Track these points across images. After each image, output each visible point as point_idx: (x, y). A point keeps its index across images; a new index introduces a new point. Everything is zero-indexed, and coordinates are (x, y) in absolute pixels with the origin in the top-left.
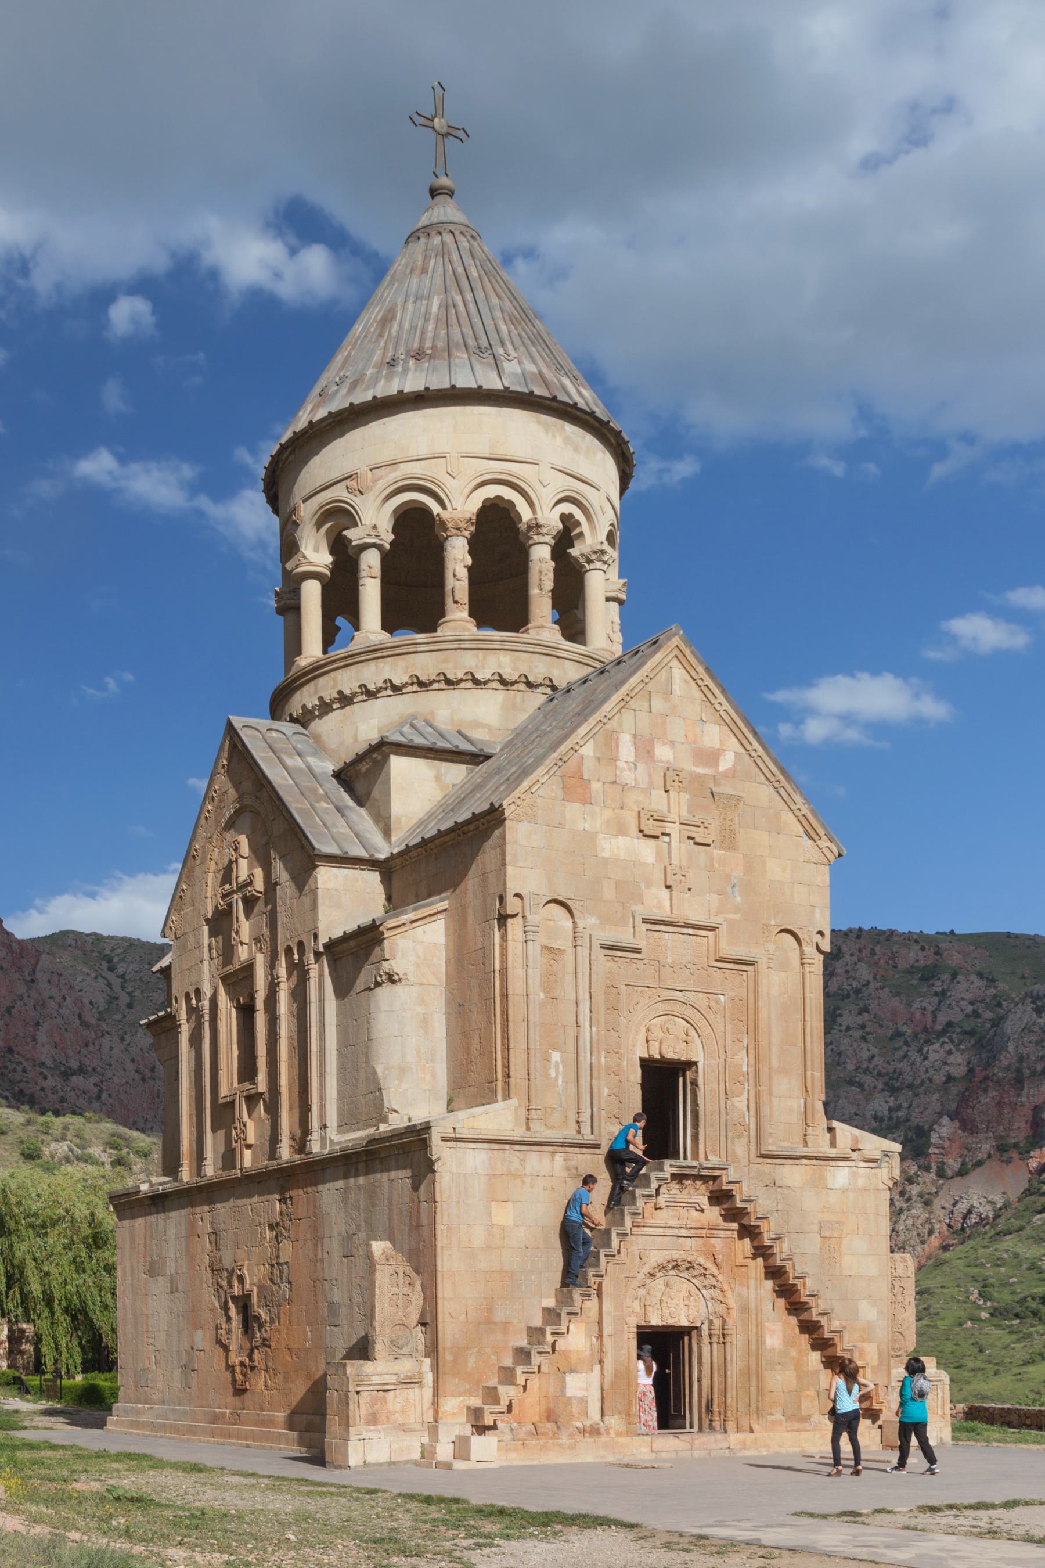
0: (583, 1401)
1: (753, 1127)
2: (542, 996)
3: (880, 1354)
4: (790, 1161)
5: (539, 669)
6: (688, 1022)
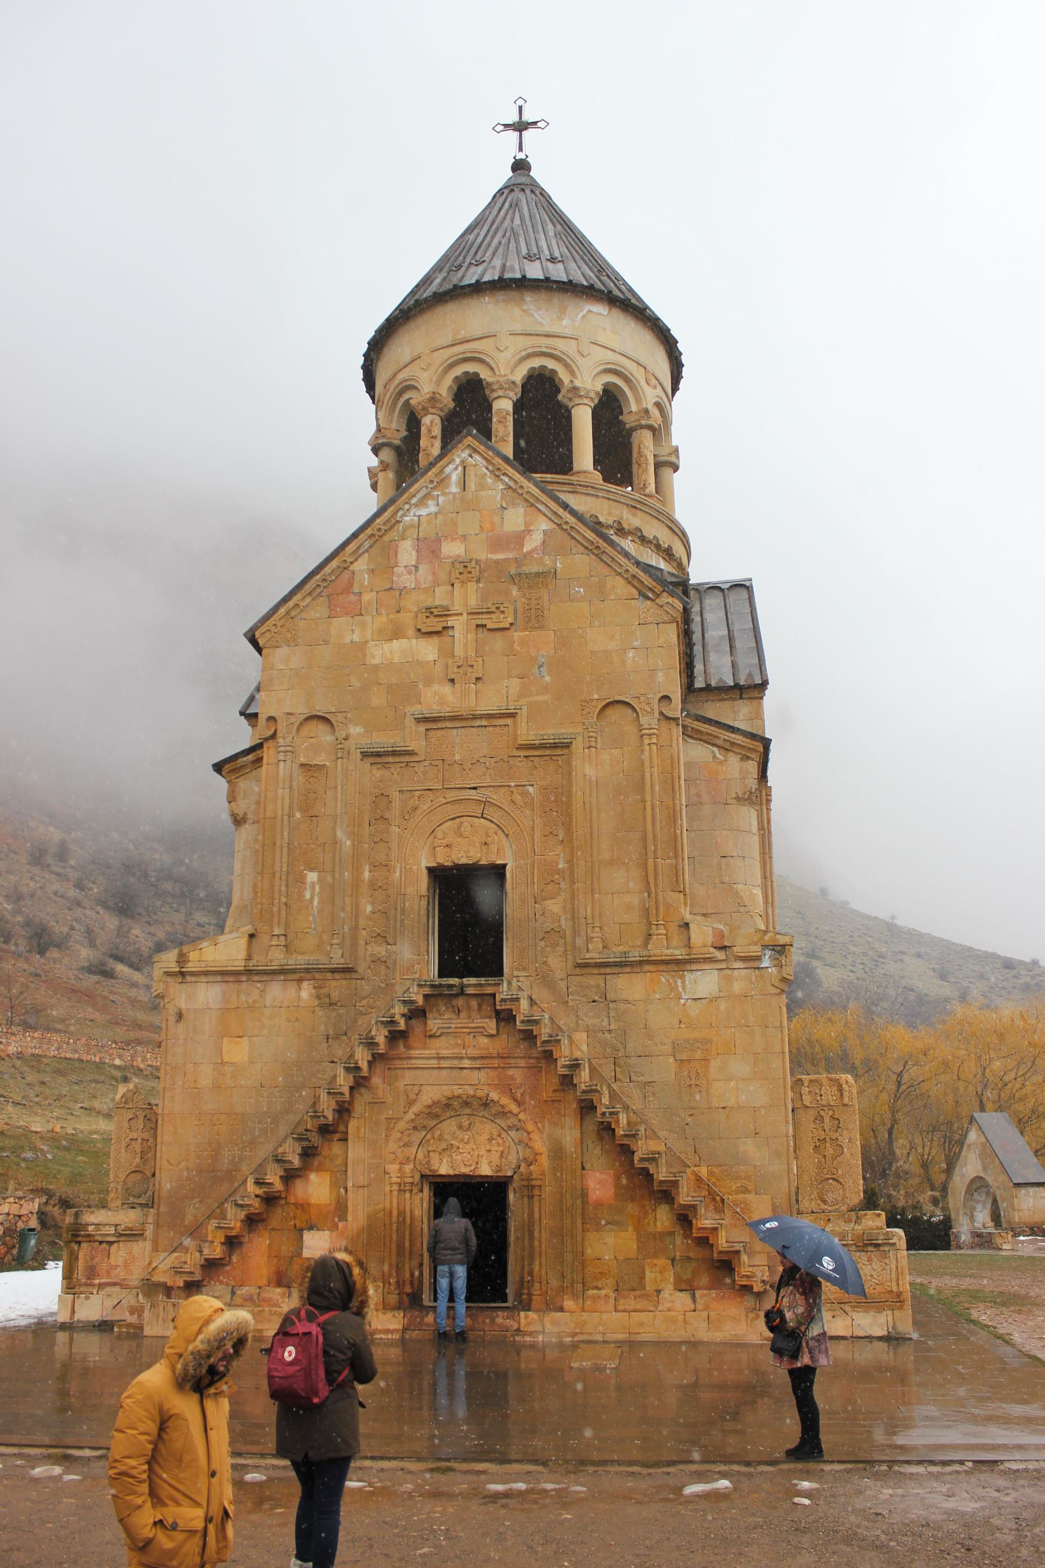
2: (298, 815)
4: (628, 969)
6: (492, 822)
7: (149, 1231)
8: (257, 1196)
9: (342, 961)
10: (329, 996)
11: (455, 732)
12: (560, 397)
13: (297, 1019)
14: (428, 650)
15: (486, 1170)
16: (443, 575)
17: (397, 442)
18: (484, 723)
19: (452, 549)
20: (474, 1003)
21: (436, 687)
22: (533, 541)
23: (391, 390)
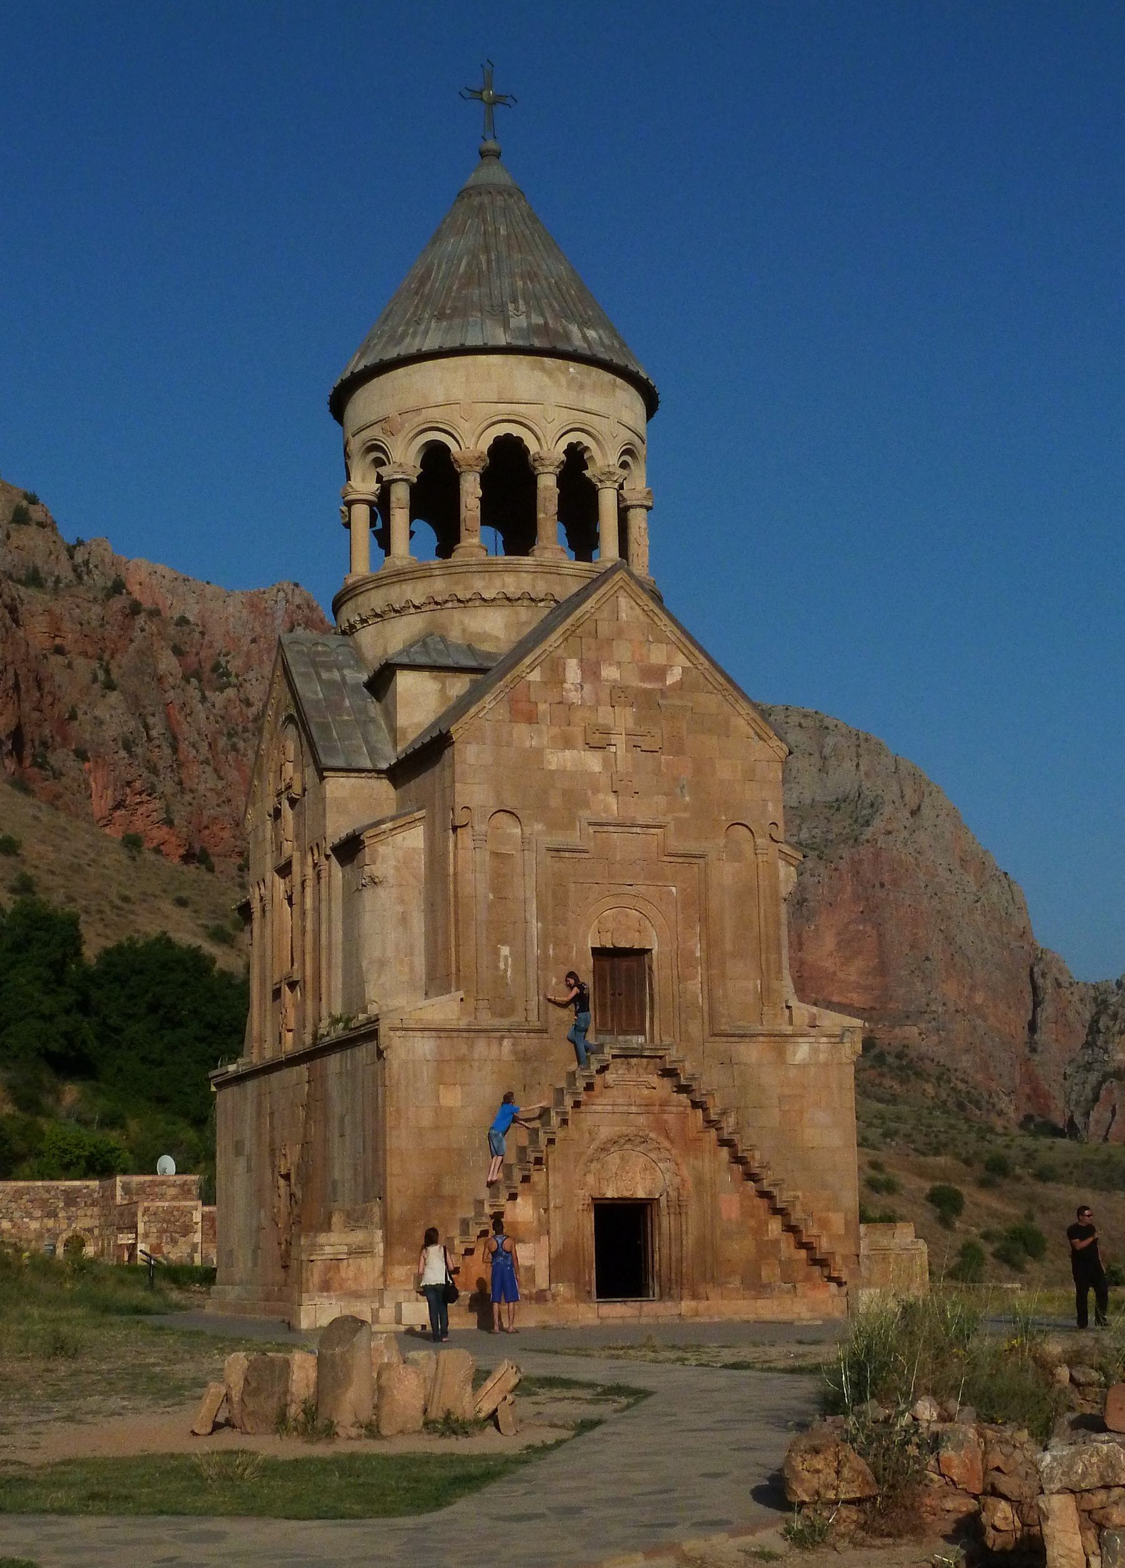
0: (531, 1270)
1: (706, 1008)
2: (491, 896)
3: (847, 1224)
4: (747, 1039)
5: (540, 588)
9: (538, 1024)
12: (588, 473)
14: (593, 762)
15: (641, 1194)
16: (605, 696)
18: (638, 830)
21: (601, 796)
22: (674, 677)
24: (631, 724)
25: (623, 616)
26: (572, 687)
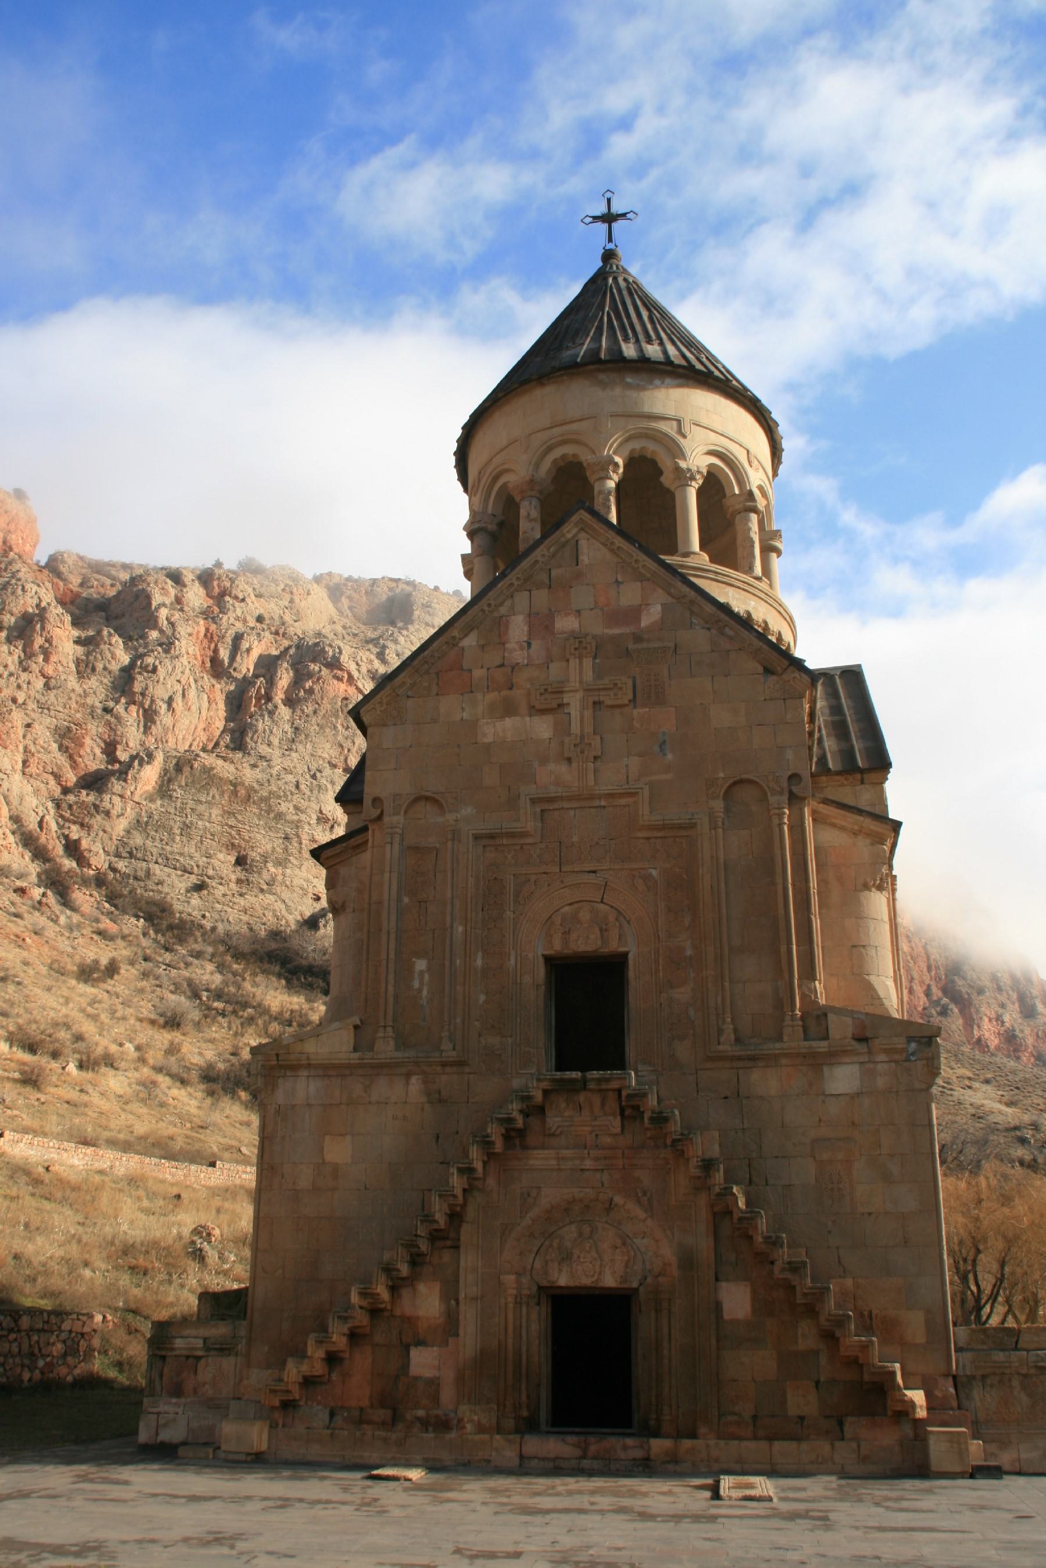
2: (406, 900)
7: (241, 1347)
8: (361, 1307)
10: (439, 1092)
11: (572, 813)
12: (663, 479)
13: (405, 1118)
14: (543, 728)
15: (610, 1281)
17: (492, 527)
19: (566, 624)
20: (597, 1100)
23: (487, 474)
24: (589, 675)
25: (584, 559)
26: (516, 646)
